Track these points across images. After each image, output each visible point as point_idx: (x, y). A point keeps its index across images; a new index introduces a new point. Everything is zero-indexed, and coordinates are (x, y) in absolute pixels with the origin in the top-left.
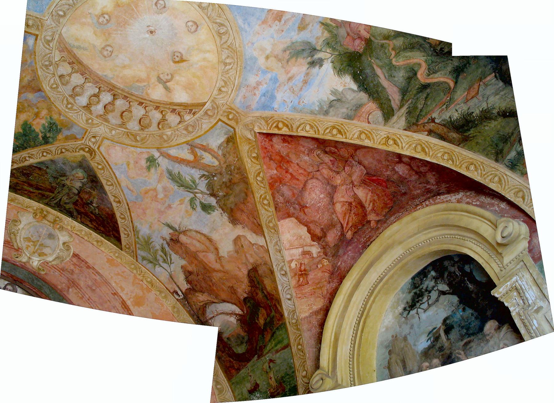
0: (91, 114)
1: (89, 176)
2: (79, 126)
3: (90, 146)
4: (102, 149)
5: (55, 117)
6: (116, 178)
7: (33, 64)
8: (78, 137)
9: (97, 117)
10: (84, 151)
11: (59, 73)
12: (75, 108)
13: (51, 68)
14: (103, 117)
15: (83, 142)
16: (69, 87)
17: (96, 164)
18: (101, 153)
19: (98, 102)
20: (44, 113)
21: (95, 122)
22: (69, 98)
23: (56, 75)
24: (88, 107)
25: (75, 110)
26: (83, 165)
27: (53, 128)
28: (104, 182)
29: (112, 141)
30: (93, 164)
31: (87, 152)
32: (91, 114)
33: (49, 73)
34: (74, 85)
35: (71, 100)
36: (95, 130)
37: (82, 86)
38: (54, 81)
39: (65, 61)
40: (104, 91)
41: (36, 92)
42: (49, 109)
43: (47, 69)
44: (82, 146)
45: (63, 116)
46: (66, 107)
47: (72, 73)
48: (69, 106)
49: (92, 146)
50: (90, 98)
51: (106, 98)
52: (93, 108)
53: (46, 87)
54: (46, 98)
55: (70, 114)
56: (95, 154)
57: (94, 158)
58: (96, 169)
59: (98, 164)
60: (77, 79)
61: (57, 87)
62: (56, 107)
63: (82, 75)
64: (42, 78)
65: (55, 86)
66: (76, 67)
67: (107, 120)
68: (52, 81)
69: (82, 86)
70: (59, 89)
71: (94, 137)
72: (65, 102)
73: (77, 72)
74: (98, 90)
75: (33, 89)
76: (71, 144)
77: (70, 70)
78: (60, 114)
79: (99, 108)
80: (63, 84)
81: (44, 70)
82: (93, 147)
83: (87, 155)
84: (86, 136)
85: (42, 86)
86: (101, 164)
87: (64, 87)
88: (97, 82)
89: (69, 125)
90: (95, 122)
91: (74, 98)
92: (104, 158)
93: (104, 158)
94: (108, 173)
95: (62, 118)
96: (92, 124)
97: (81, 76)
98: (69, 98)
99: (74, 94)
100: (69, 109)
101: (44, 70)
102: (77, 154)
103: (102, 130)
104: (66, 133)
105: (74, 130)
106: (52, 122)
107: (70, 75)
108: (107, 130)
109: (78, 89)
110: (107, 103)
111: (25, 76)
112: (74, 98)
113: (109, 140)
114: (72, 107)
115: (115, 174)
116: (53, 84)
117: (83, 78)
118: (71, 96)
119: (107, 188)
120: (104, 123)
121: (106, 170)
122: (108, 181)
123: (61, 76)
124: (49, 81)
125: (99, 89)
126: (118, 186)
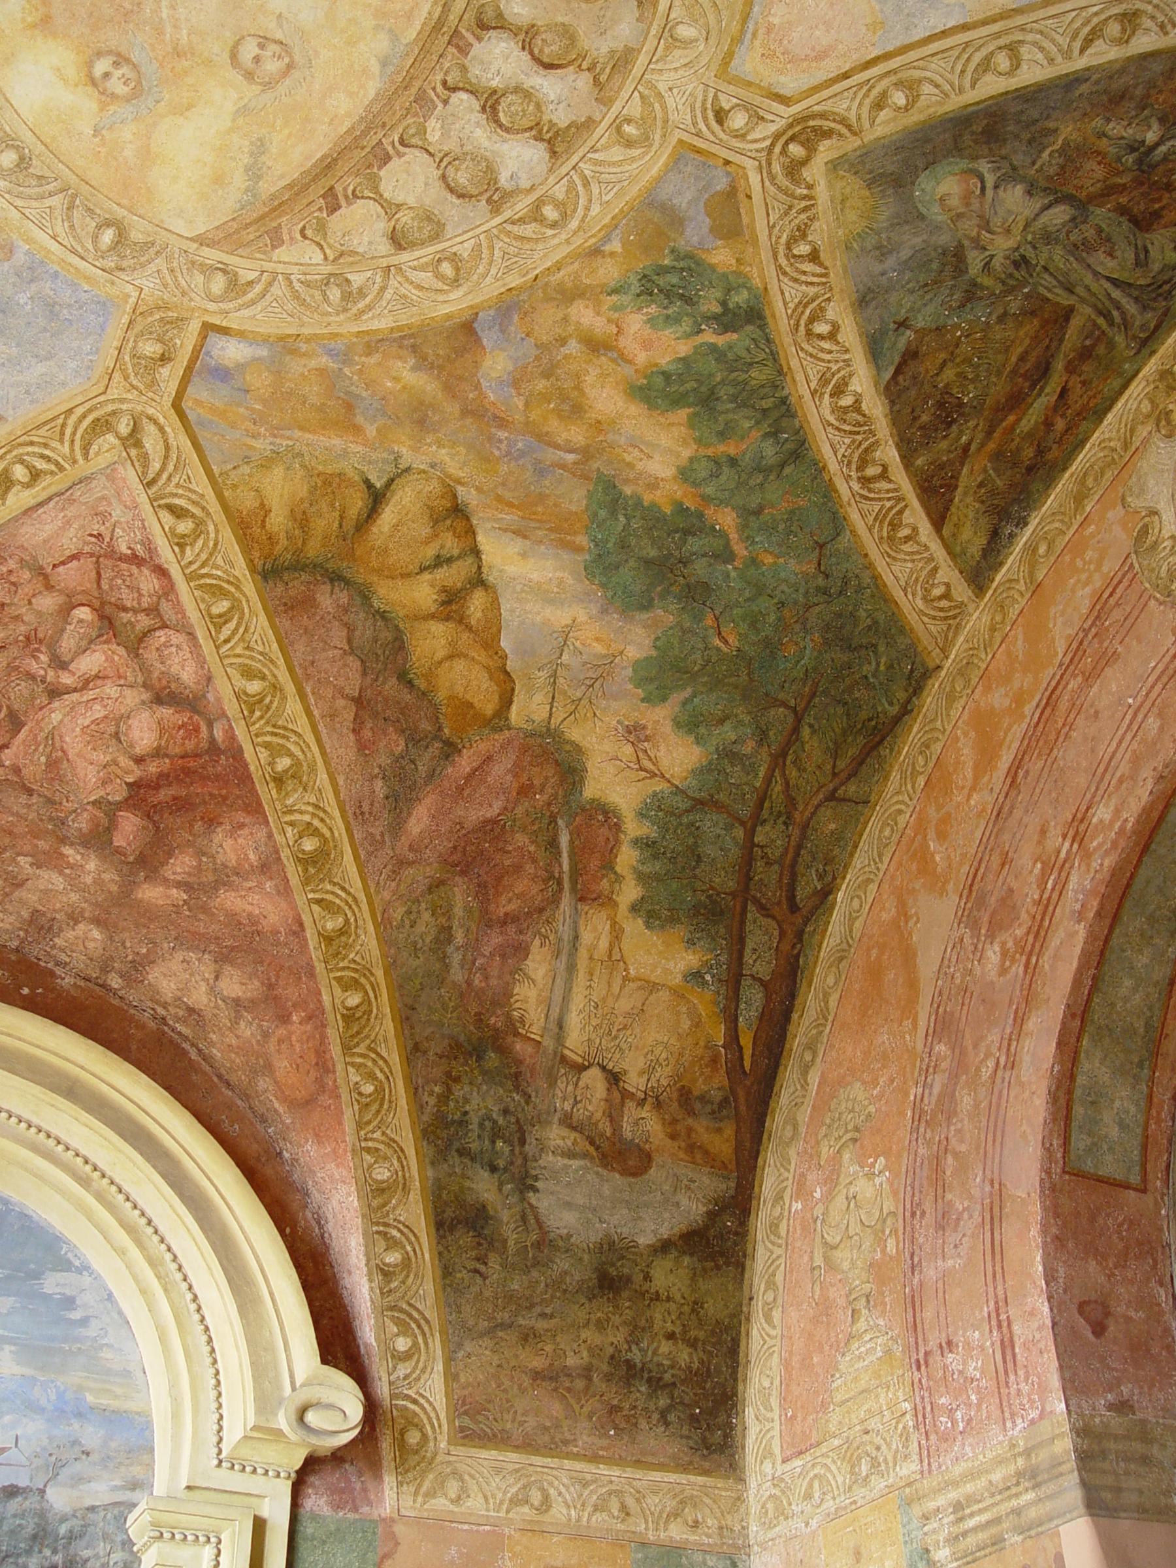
0: (589, 124)
1: (957, 149)
2: (659, 180)
3: (777, 136)
4: (789, 84)
5: (608, 272)
6: (965, 27)
7: (339, 345)
8: (721, 184)
9: (607, 102)
10: (804, 162)
11: (384, 247)
12: (559, 192)
13: (357, 279)
14: (607, 74)
15: (749, 164)
16: (451, 210)
17: (884, 115)
18: (816, 89)
19: (527, 95)
20: (584, 315)
21: (635, 109)
22: (507, 214)
23: (395, 260)
24: (556, 141)
25: (571, 187)
26: (896, 168)
27: (670, 282)
28: (992, 86)
29: (738, 40)
30: (885, 126)
31: (811, 150)
32: (589, 124)
33: (383, 289)
34: (437, 190)
35: (521, 206)
36: (678, 109)
37: (445, 161)
38: (423, 268)
39: (322, 228)
40: (464, 69)
41: (478, 340)
42: (569, 295)
43: (362, 293)
44: (777, 168)
45: (607, 239)
46: (554, 225)
47: (379, 199)
48: (550, 213)
49: (773, 128)
50: (507, 130)
51: (499, 61)
52: (562, 118)
53: (454, 303)
54: (508, 307)
55: (595, 210)
56: (823, 116)
57: (844, 122)
58: (915, 117)
59: (879, 105)
60: (409, 180)
61: (454, 259)
62: (558, 266)
63: (387, 159)
64: (406, 317)
65: (447, 269)
66: (351, 183)
67: (623, 60)
68: (426, 278)
69: (445, 161)
70: (465, 251)
71: (720, 116)
72: (529, 230)
73: (374, 183)
74: (464, 96)
75: (460, 352)
76: (762, 215)
77: (364, 209)
78: (595, 252)
79: (560, 94)
80: (436, 237)
81: (369, 308)
82: (780, 124)
83: (826, 150)
84: (715, 149)
85: (449, 317)
86: (884, 95)
87: (449, 231)
88: (420, 98)
89: (654, 217)
90: (635, 109)
91: (507, 195)
92: (846, 76)
93: (846, 76)
94: (935, 64)
95: (616, 246)
96: (646, 122)
97: (395, 163)
98: (507, 214)
99: (492, 193)
100: (565, 216)
101: (369, 308)
102: (822, 192)
103: (678, 85)
104: (696, 233)
105: (684, 195)
106: (636, 288)
107: (391, 209)
108: (679, 57)
109: (462, 178)
110: (525, 56)
111: (396, 379)
112: (507, 195)
113: (730, 55)
114: (557, 205)
115: (944, 34)
116: (439, 276)
117: (400, 155)
118: (495, 207)
119: (1032, 73)
120: (637, 71)
121: (917, 74)
122: (986, 65)
123: (398, 240)
124: (420, 287)
125: (455, 89)
126: (1019, 20)
